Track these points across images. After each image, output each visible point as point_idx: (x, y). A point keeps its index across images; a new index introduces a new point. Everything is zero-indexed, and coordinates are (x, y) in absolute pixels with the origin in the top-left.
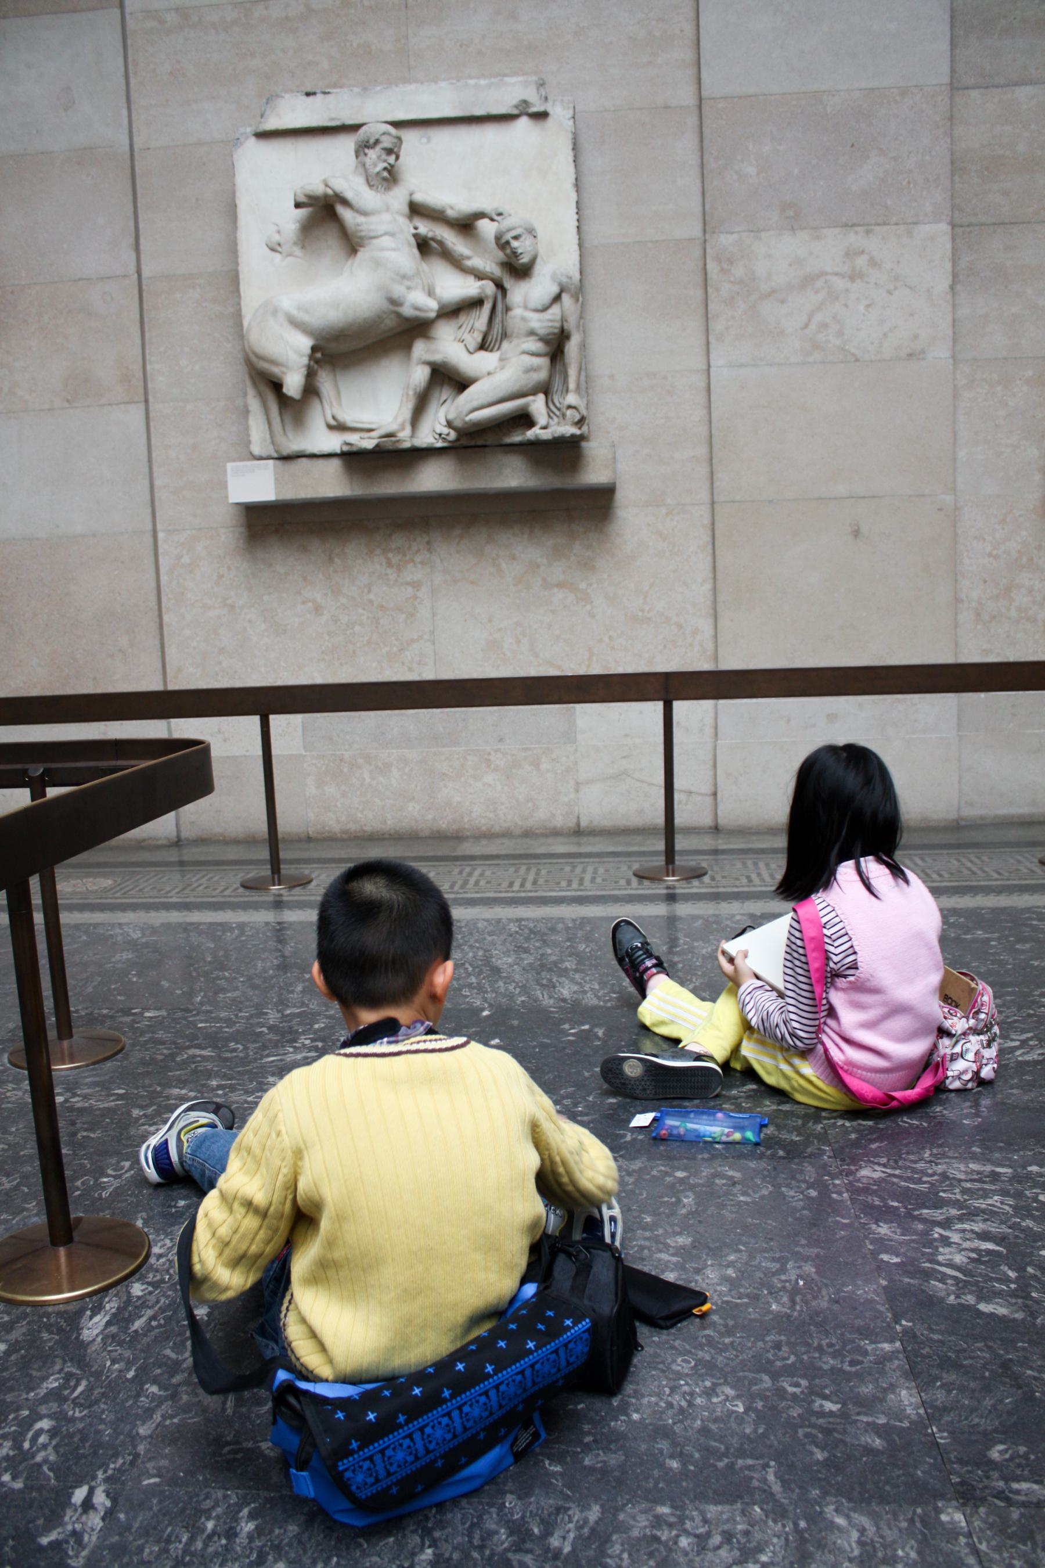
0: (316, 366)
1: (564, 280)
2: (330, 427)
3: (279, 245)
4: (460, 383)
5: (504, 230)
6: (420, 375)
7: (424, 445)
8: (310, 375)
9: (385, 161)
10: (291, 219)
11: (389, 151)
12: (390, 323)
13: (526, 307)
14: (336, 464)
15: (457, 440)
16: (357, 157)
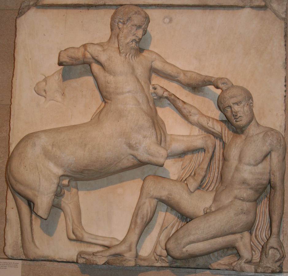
9: (134, 35)
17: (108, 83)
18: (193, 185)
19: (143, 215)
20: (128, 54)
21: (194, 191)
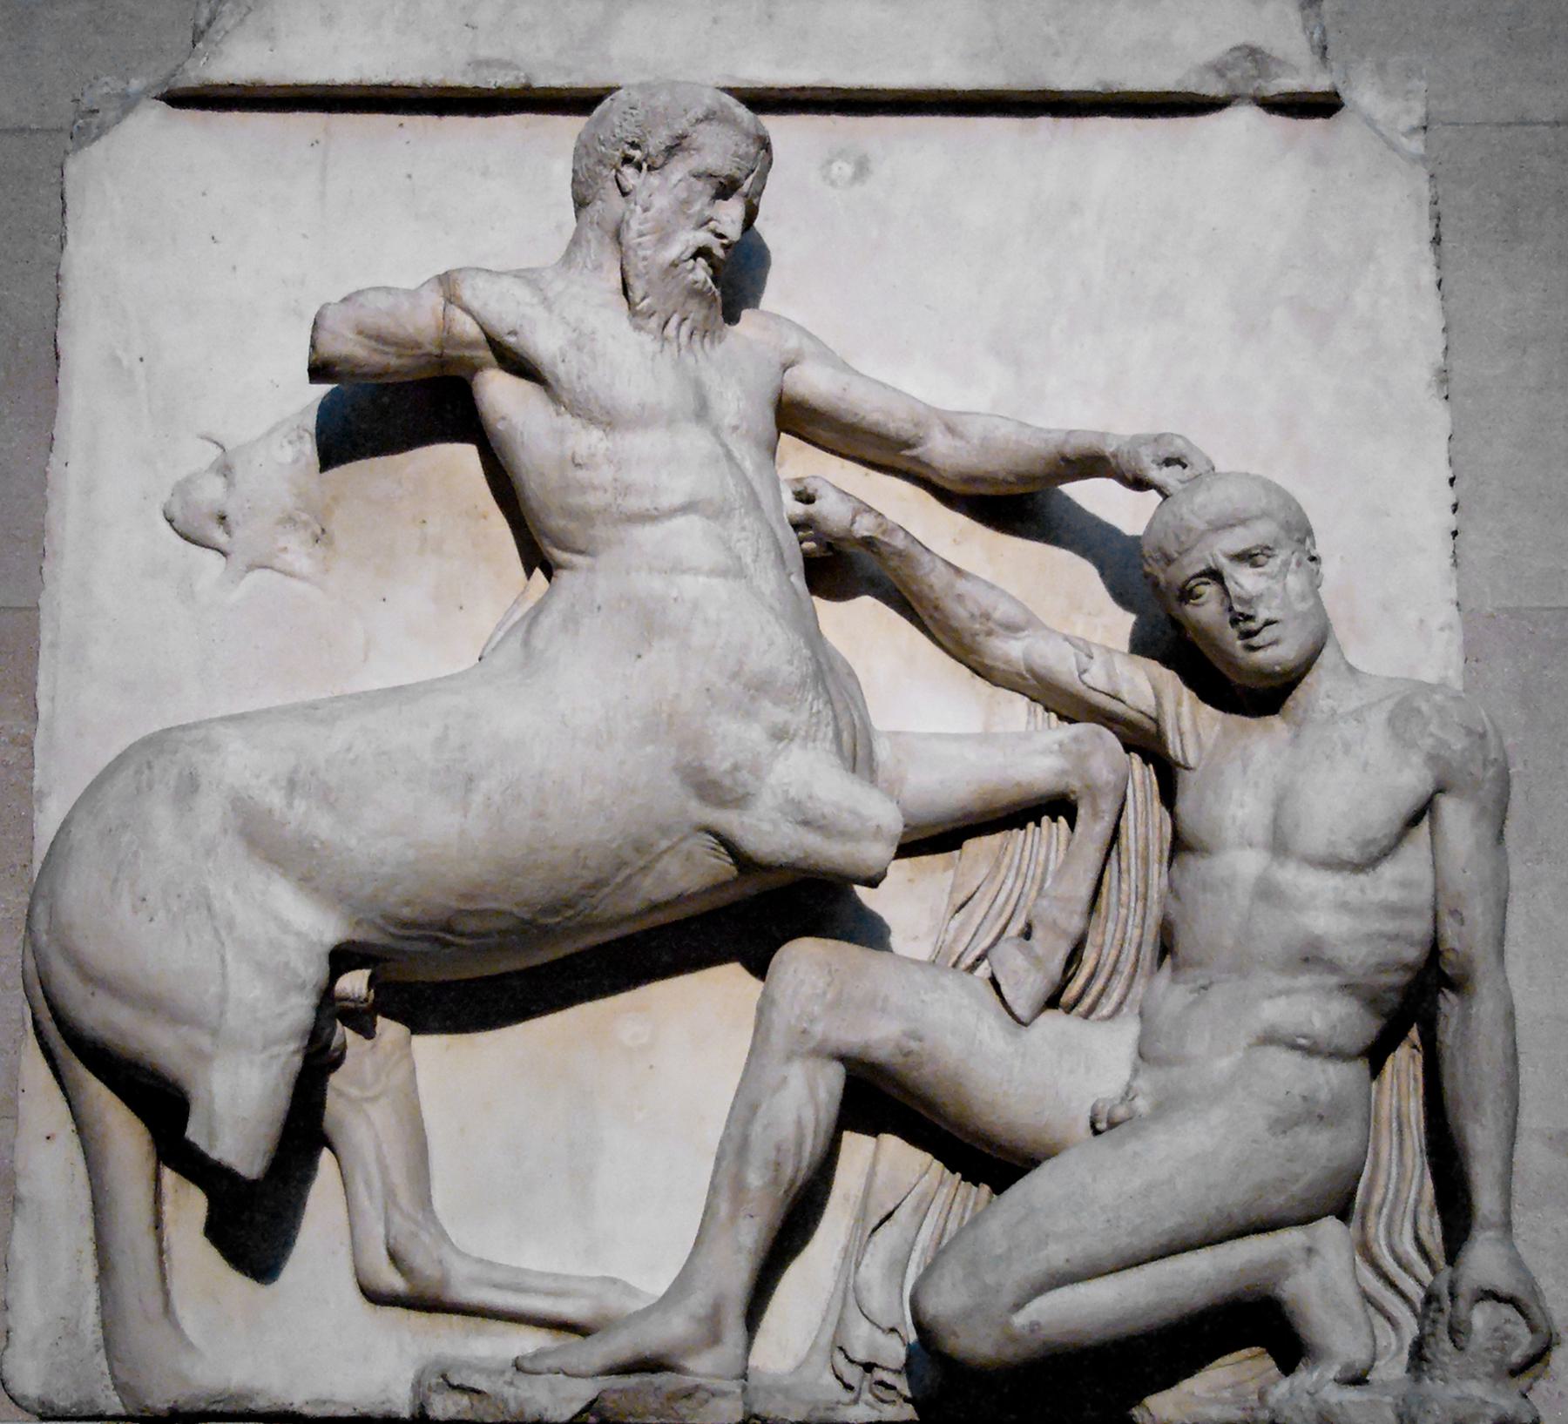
2: (374, 1296)
4: (988, 1159)
8: (317, 1065)
12: (688, 872)
16: (581, 204)
17: (578, 465)
18: (1026, 980)
19: (778, 1149)
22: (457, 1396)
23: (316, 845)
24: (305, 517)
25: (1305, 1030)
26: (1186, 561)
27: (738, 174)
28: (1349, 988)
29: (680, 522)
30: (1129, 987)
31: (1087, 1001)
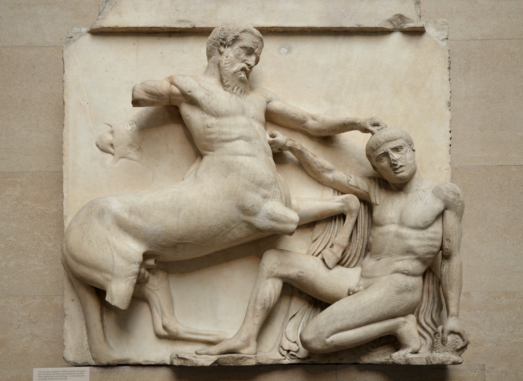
0: (147, 273)
1: (451, 197)
2: (159, 337)
3: (112, 145)
5: (383, 141)
6: (271, 289)
7: (270, 362)
8: (140, 282)
9: (244, 61)
10: (126, 117)
11: (250, 51)
12: (239, 233)
13: (402, 223)
14: (164, 374)
15: (308, 357)
16: (209, 57)
17: (208, 127)
19: (265, 300)
20: (236, 88)
21: (334, 267)
22: (181, 360)
23: (138, 227)
24: (135, 144)
25: (407, 269)
26: (378, 150)
27: (253, 47)
28: (419, 259)
29: (237, 142)
30: (359, 260)
31: (347, 263)
